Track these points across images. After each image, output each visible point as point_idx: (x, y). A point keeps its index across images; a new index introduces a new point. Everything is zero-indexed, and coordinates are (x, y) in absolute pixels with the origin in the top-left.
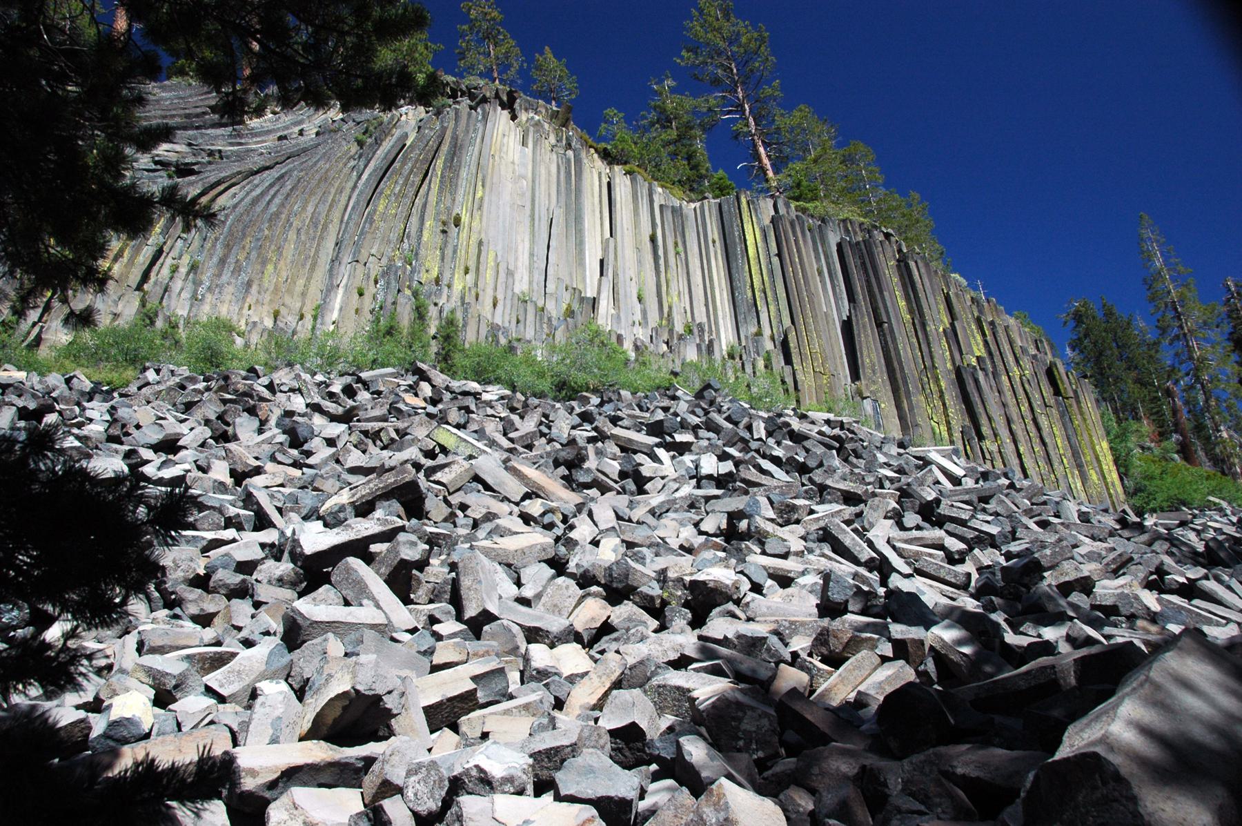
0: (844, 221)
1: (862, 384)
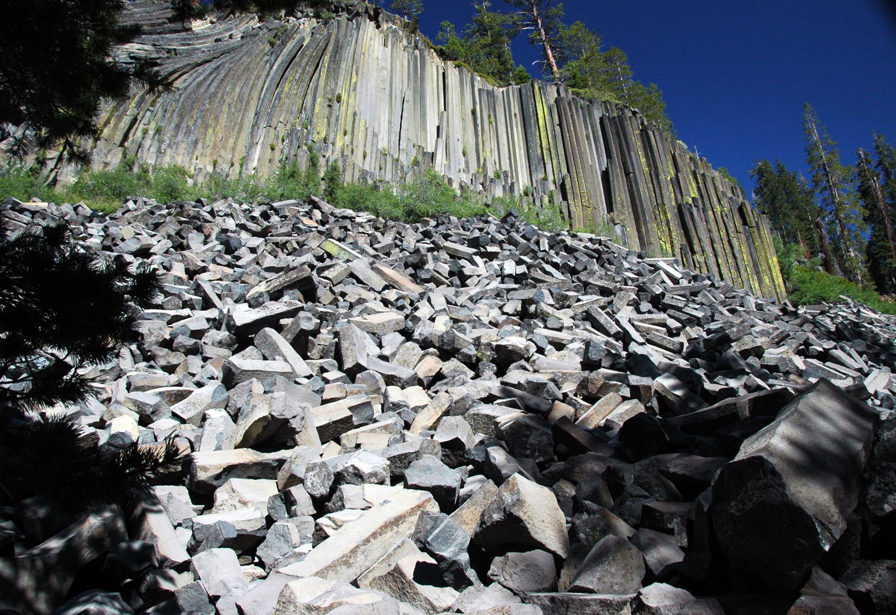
0: (605, 102)
1: (615, 214)
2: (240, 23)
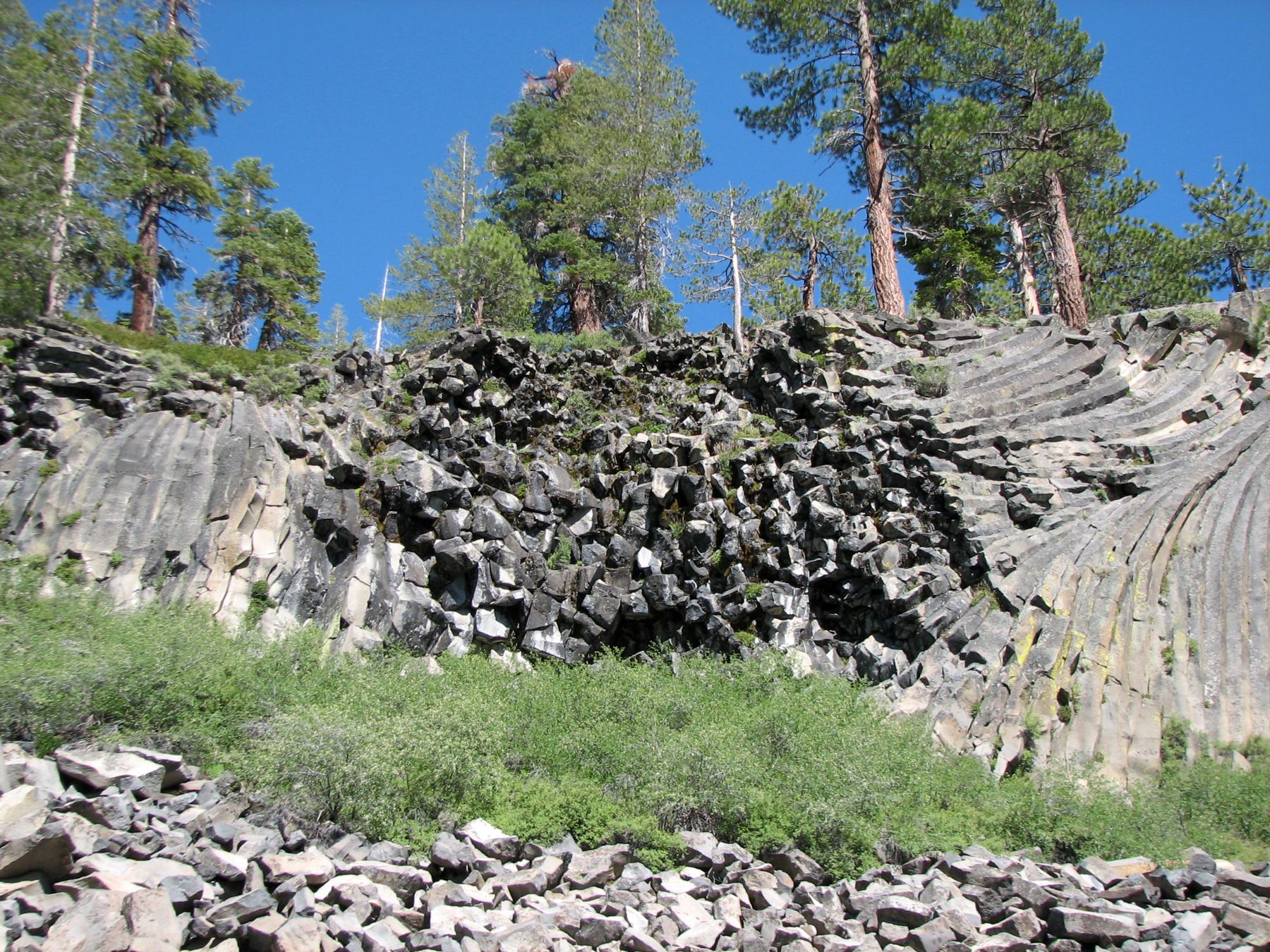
2: (1209, 366)
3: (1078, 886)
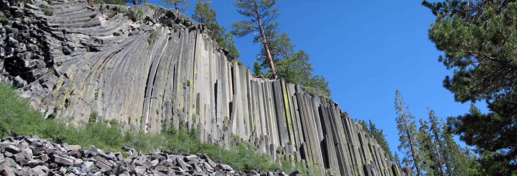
0: (320, 97)
2: (123, 22)
3: (60, 150)
